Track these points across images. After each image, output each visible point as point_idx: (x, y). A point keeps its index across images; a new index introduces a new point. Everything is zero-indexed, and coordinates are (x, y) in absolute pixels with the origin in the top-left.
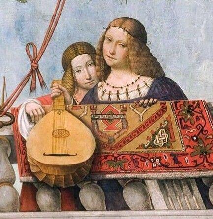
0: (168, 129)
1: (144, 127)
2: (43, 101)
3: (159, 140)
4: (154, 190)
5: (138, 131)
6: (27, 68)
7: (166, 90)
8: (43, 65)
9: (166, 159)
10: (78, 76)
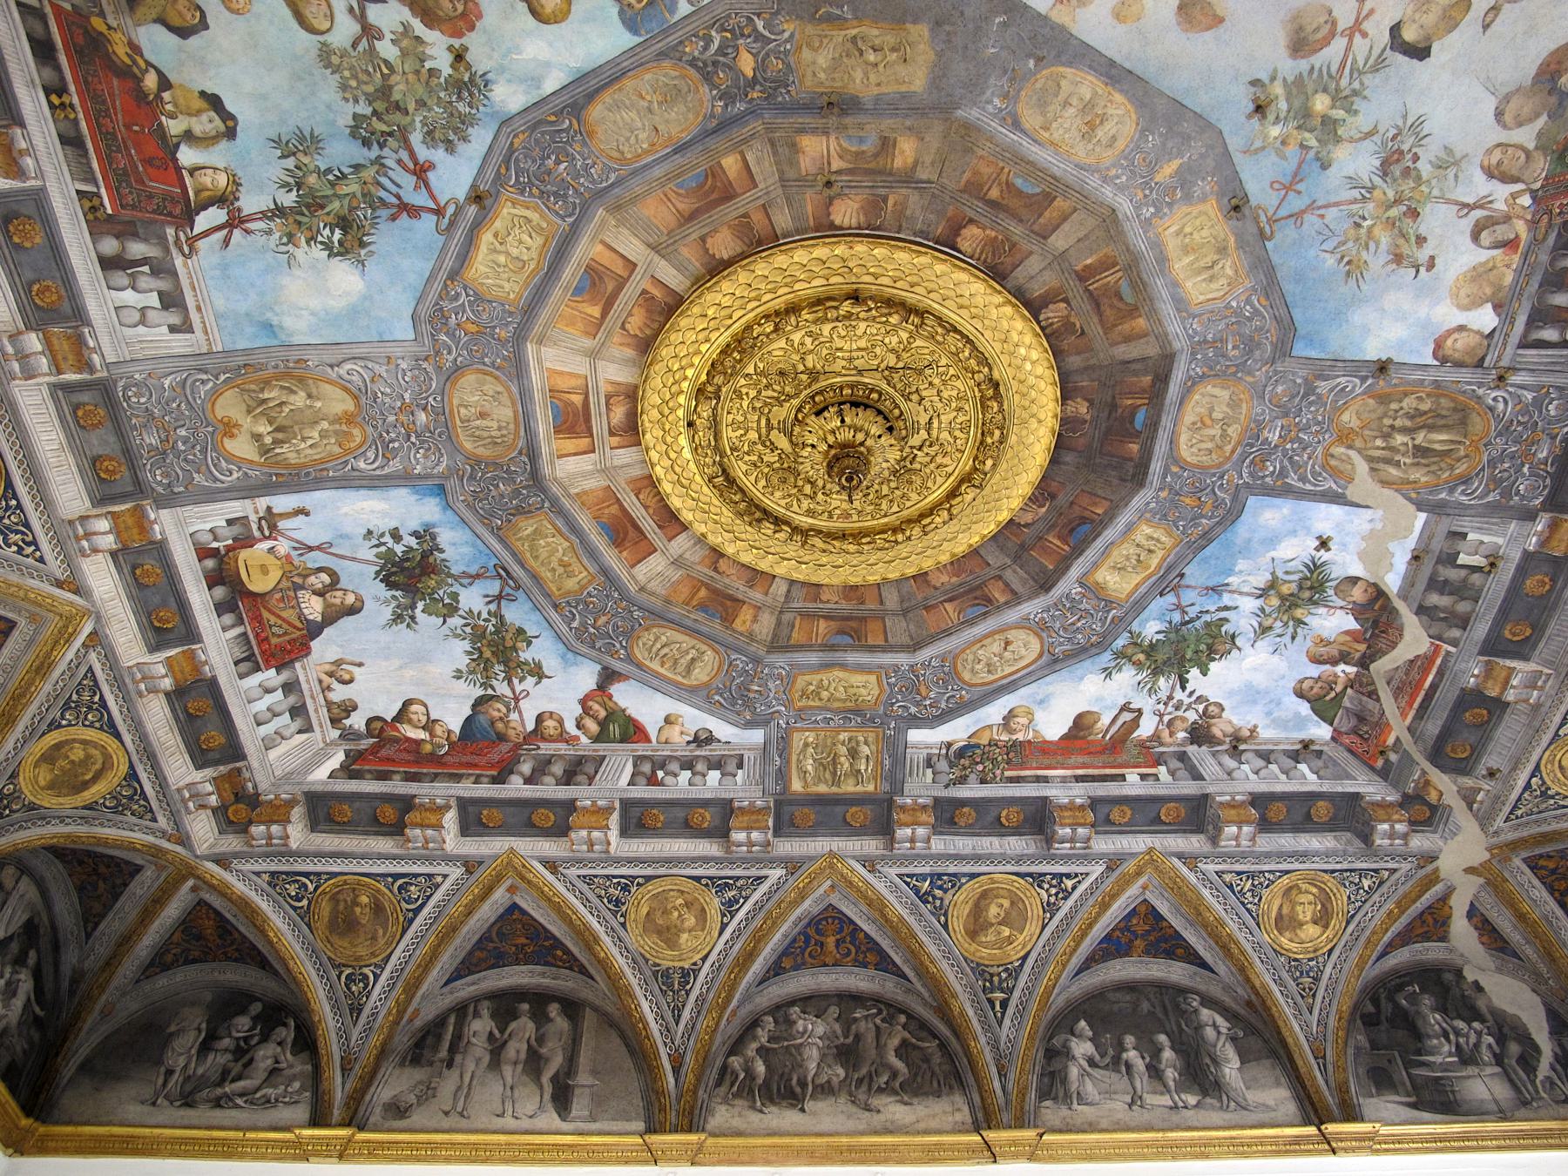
0: (285, 634)
1: (284, 620)
2: (288, 556)
3: (274, 629)
4: (238, 630)
5: (279, 617)
7: (314, 630)
8: (317, 552)
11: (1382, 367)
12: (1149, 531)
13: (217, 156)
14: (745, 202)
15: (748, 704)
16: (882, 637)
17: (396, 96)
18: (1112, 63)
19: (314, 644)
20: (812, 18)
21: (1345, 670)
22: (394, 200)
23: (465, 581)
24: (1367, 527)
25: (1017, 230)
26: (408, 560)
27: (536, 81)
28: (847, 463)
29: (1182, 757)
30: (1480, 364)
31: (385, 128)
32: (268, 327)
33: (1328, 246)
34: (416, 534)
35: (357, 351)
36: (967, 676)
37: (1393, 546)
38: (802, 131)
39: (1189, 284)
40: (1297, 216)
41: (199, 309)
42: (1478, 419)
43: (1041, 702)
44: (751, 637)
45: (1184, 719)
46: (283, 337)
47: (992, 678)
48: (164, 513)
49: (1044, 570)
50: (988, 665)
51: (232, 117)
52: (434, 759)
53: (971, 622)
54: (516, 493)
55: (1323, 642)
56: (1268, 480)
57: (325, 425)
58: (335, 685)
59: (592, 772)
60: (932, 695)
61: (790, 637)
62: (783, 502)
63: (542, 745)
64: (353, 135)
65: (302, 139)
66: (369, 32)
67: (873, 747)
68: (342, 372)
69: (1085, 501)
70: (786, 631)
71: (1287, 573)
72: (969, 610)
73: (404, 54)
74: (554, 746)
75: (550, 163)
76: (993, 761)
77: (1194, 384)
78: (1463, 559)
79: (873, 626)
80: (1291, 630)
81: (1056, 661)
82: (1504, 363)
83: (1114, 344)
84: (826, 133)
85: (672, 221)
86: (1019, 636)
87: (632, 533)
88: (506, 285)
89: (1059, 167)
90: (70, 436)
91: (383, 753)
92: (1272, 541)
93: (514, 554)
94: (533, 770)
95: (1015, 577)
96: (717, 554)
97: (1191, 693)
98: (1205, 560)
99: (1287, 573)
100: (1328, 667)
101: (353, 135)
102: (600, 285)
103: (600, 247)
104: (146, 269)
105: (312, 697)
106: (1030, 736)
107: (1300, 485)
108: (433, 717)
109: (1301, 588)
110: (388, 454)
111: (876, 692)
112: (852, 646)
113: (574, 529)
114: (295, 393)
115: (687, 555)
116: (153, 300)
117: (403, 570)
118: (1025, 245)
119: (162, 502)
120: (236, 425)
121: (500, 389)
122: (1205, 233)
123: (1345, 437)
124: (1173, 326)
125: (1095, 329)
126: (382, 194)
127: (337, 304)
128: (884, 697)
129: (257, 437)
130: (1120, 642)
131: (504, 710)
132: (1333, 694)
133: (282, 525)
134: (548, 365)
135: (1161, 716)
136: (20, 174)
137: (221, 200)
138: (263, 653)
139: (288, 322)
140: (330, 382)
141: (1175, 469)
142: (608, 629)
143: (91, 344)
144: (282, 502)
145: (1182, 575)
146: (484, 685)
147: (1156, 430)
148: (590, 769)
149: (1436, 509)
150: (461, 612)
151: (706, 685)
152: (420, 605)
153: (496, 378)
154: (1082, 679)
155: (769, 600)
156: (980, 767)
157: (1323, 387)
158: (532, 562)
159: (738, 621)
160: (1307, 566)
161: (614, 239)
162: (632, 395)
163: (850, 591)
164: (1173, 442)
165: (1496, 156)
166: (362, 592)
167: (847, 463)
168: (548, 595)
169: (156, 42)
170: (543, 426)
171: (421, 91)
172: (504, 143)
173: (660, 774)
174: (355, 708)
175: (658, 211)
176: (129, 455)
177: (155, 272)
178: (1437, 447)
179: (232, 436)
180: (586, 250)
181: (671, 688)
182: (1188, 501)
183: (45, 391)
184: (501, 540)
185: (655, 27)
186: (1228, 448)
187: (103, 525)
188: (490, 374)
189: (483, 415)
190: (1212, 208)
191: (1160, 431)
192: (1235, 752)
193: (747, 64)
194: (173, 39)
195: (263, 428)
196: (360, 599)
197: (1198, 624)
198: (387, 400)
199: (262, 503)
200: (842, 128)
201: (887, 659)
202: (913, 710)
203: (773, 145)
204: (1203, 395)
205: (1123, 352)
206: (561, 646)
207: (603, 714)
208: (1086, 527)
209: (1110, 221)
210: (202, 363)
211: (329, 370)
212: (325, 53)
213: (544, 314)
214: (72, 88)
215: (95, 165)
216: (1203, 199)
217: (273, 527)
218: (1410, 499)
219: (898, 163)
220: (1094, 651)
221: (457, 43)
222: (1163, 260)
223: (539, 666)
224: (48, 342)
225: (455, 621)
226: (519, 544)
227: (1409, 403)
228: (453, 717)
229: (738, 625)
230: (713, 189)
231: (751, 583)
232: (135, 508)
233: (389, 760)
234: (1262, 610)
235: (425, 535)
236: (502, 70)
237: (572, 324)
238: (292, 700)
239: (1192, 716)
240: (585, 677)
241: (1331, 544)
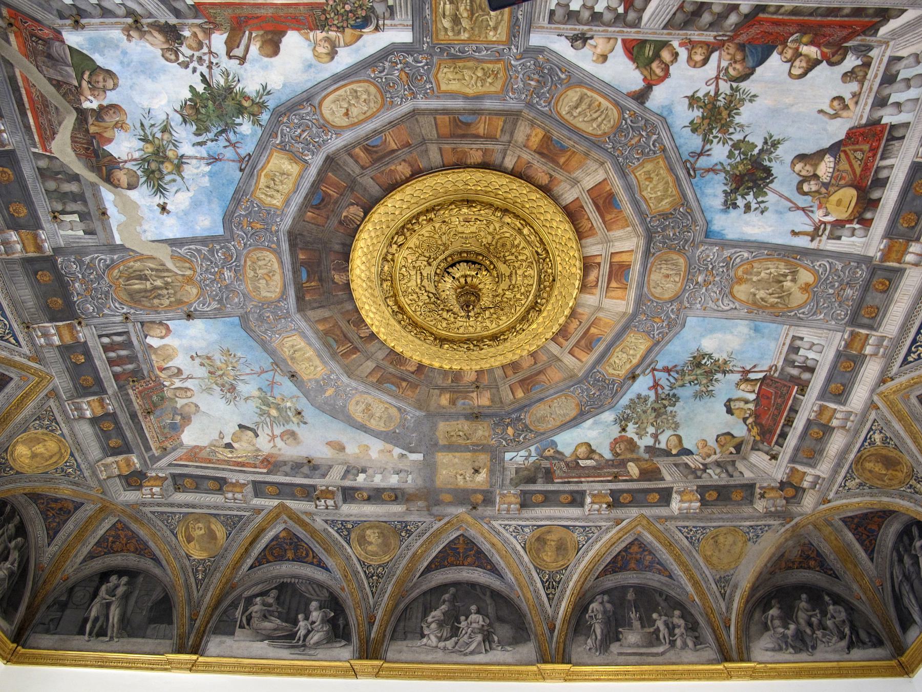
0: (855, 151)
2: (820, 207)
3: (859, 155)
5: (851, 165)
6: (801, 213)
7: (835, 149)
8: (801, 205)
9: (870, 154)
10: (813, 189)
11: (189, 316)
12: (275, 202)
13: (740, 394)
14: (514, 379)
15: (539, 68)
16: (439, 122)
17: (654, 415)
18: (365, 432)
19: (842, 136)
20: (484, 445)
21: (91, 103)
22: (672, 373)
23: (719, 167)
24: (145, 227)
25: (391, 369)
26: (749, 188)
27: (595, 423)
28: (469, 297)
29: (177, 13)
30: (142, 324)
31: (664, 402)
32: (756, 330)
33: (242, 360)
34: (735, 206)
35: (719, 314)
36: (372, 89)
37: (123, 218)
38: (489, 407)
39: (303, 344)
40: (263, 372)
41: (784, 344)
42: (124, 298)
43: (310, 66)
44: (532, 124)
45: (190, 47)
46: (752, 325)
47: (354, 86)
48: (871, 254)
49: (333, 171)
50: (357, 97)
51: (725, 405)
52: (804, 28)
53: (376, 132)
54: (663, 230)
55: (120, 125)
56: (218, 247)
57: (755, 279)
58: (847, 96)
59: (679, 15)
60: (396, 73)
61: (505, 122)
62: (505, 229)
63: (711, 39)
64: (679, 398)
65: (701, 397)
66: (655, 436)
67: (439, 26)
68: (732, 306)
69: (320, 220)
70: (507, 127)
71: (174, 181)
72: (379, 143)
73: (645, 429)
74: (703, 39)
75: (598, 393)
76: (337, 13)
77: (282, 297)
78: (75, 217)
79: (445, 131)
80: (148, 133)
81: (308, 100)
82: (130, 325)
83: (331, 317)
84: (479, 406)
85: (549, 371)
86: (338, 120)
87: (601, 202)
88: (633, 340)
89: (377, 393)
90: (887, 308)
91: (845, 33)
92: (196, 204)
93: (680, 185)
94: (727, 17)
95: (353, 168)
96: (546, 190)
97: (194, 70)
98: (230, 182)
99: (174, 181)
100: (105, 103)
101: (679, 398)
102: (588, 342)
103: (584, 360)
104: (796, 364)
105: (871, 89)
106: (311, 34)
107: (199, 247)
108: (789, 64)
109: (160, 170)
110: (728, 262)
111: (440, 75)
112: (460, 114)
113: (635, 203)
114: (762, 299)
115: (568, 187)
116: (802, 352)
117: (754, 182)
118: (386, 363)
119: (867, 260)
120: (800, 288)
121: (653, 290)
122: (304, 366)
123: (189, 280)
124: (303, 324)
125: (343, 324)
126: (676, 376)
127: (719, 335)
128: (434, 71)
129: (794, 280)
130: (265, 117)
131: (731, 71)
132: (86, 76)
133: (810, 229)
134: (624, 302)
135: (211, 52)
136: (821, 406)
137: (747, 380)
138: (880, 140)
139: (745, 330)
140: (740, 301)
141: (274, 246)
142: (634, 130)
143: (843, 343)
144: (803, 242)
145: (241, 170)
146: (737, 90)
147: (293, 268)
148: (680, 17)
149: (114, 248)
150: (730, 143)
151: (569, 87)
152: (756, 151)
153: (653, 295)
154: (284, 85)
155: (518, 152)
156: (348, 7)
157: (215, 305)
158: (670, 179)
159: (540, 136)
160: (165, 189)
161: (576, 363)
162: (584, 288)
163: (460, 165)
164: (281, 263)
165: (189, 394)
166: (789, 169)
167: (469, 297)
168: (667, 159)
169: (740, 431)
170: (637, 268)
171: (643, 416)
172: (615, 400)
173: (621, 10)
174: (845, 74)
175: (554, 375)
176: (867, 287)
177: (794, 362)
178: (137, 282)
179: (808, 285)
180: (589, 359)
181: (597, 85)
182: (258, 226)
183: (881, 329)
184: (684, 196)
185: (544, 442)
186: (249, 263)
187: (909, 258)
188: (655, 297)
189: (667, 276)
190: (305, 378)
191: (290, 268)
192: (130, 13)
193: (510, 431)
194: (732, 432)
195: (787, 284)
196: (793, 164)
197: (215, 131)
198: (715, 289)
199: (813, 245)
200: (472, 408)
201: (434, 104)
202: (410, 59)
203: (501, 402)
204: (275, 291)
205: (325, 313)
206: (669, 120)
207: (654, 66)
208: (315, 202)
209: (350, 374)
210: (798, 321)
211: (738, 307)
212: (677, 426)
213: (618, 328)
214: (781, 424)
215: (790, 402)
216: (310, 380)
217: (817, 229)
218: (133, 251)
219: (448, 396)
220: (282, 109)
221: (623, 434)
222: (319, 356)
223: (691, 106)
224: (863, 347)
225: (737, 137)
226: (674, 193)
227: (166, 302)
228: (775, 63)
229: (540, 133)
230: (528, 384)
231: (529, 165)
232: (885, 261)
233: (842, 26)
234: (175, 146)
235: (730, 205)
236: (607, 426)
237: (606, 323)
238: (886, 92)
239: (184, 49)
240: (659, 96)
241: (160, 210)
